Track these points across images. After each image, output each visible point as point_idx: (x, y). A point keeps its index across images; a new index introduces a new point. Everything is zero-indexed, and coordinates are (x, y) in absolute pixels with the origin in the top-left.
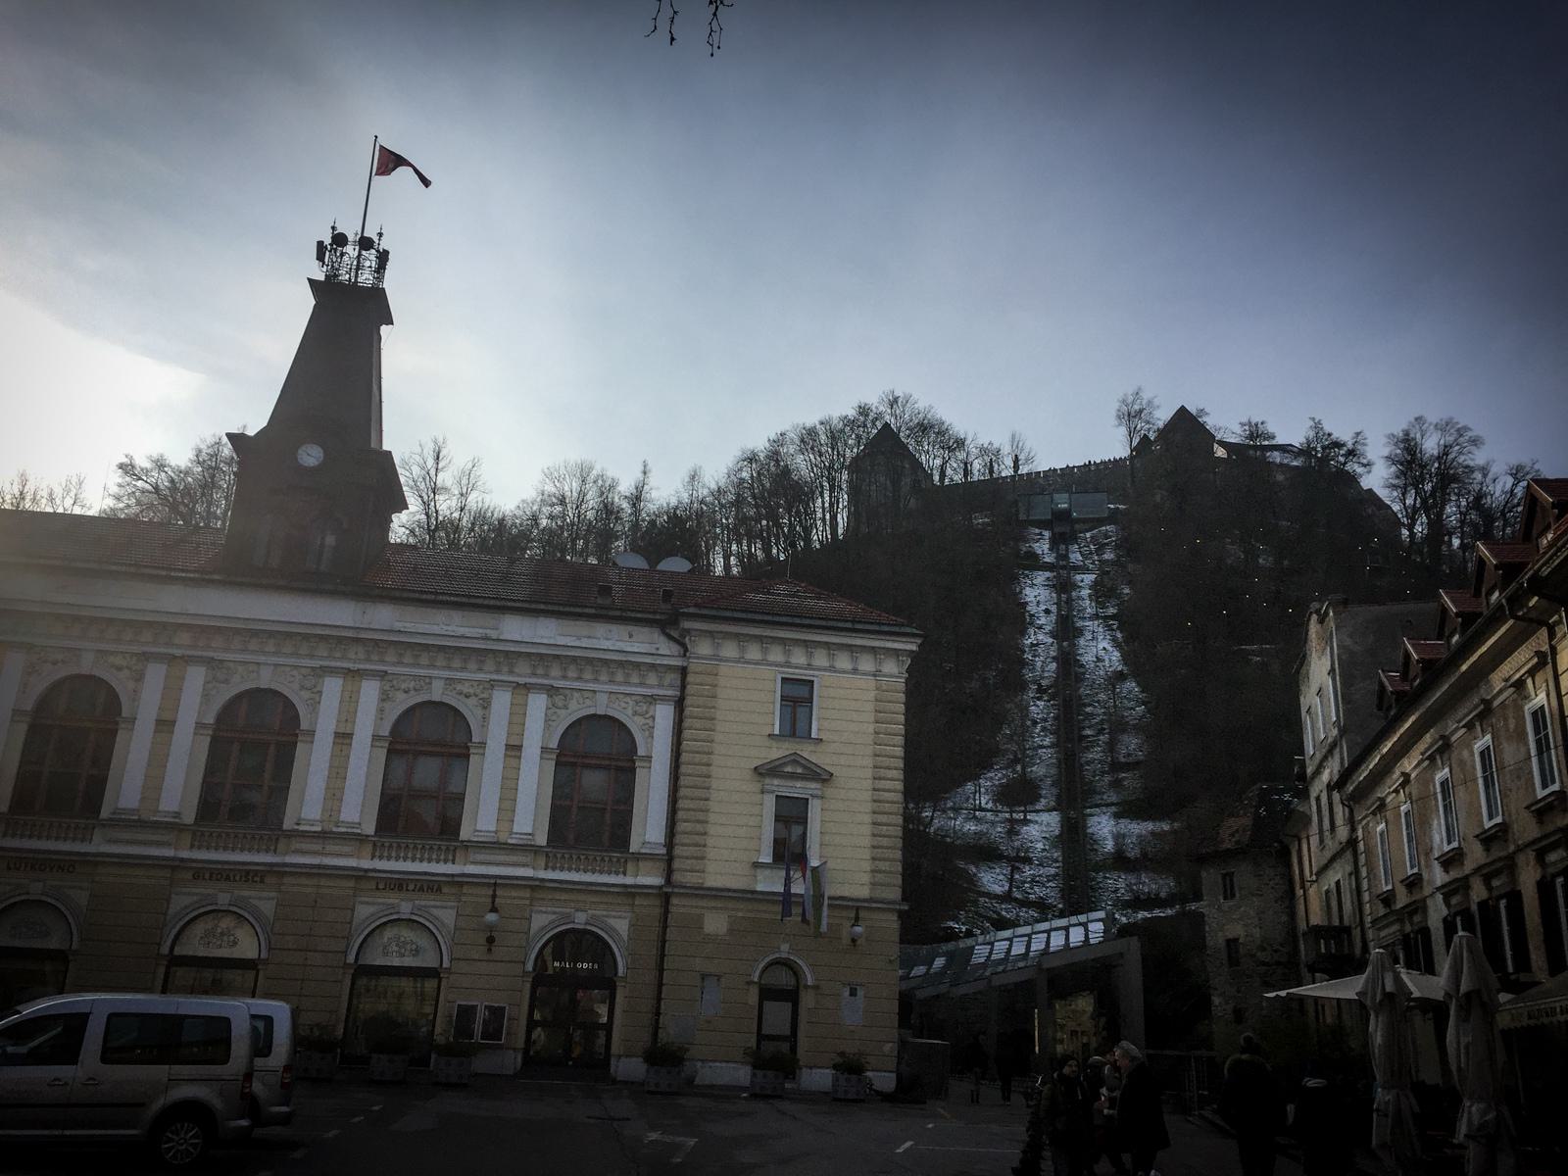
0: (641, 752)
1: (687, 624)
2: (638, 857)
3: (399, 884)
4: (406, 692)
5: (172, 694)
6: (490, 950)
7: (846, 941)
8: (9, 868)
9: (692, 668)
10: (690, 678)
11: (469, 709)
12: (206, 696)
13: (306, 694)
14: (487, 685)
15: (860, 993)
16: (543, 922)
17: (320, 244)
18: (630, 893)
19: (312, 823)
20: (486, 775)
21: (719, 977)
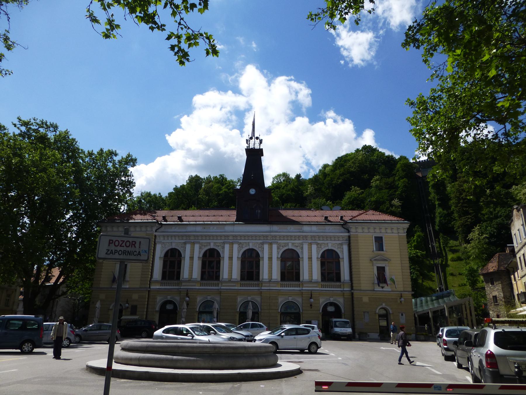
0: (341, 256)
7: (399, 302)
9: (351, 236)
10: (351, 239)
11: (298, 250)
12: (239, 252)
13: (260, 249)
15: (404, 315)
16: (323, 301)
17: (247, 140)
19: (266, 279)
21: (368, 313)
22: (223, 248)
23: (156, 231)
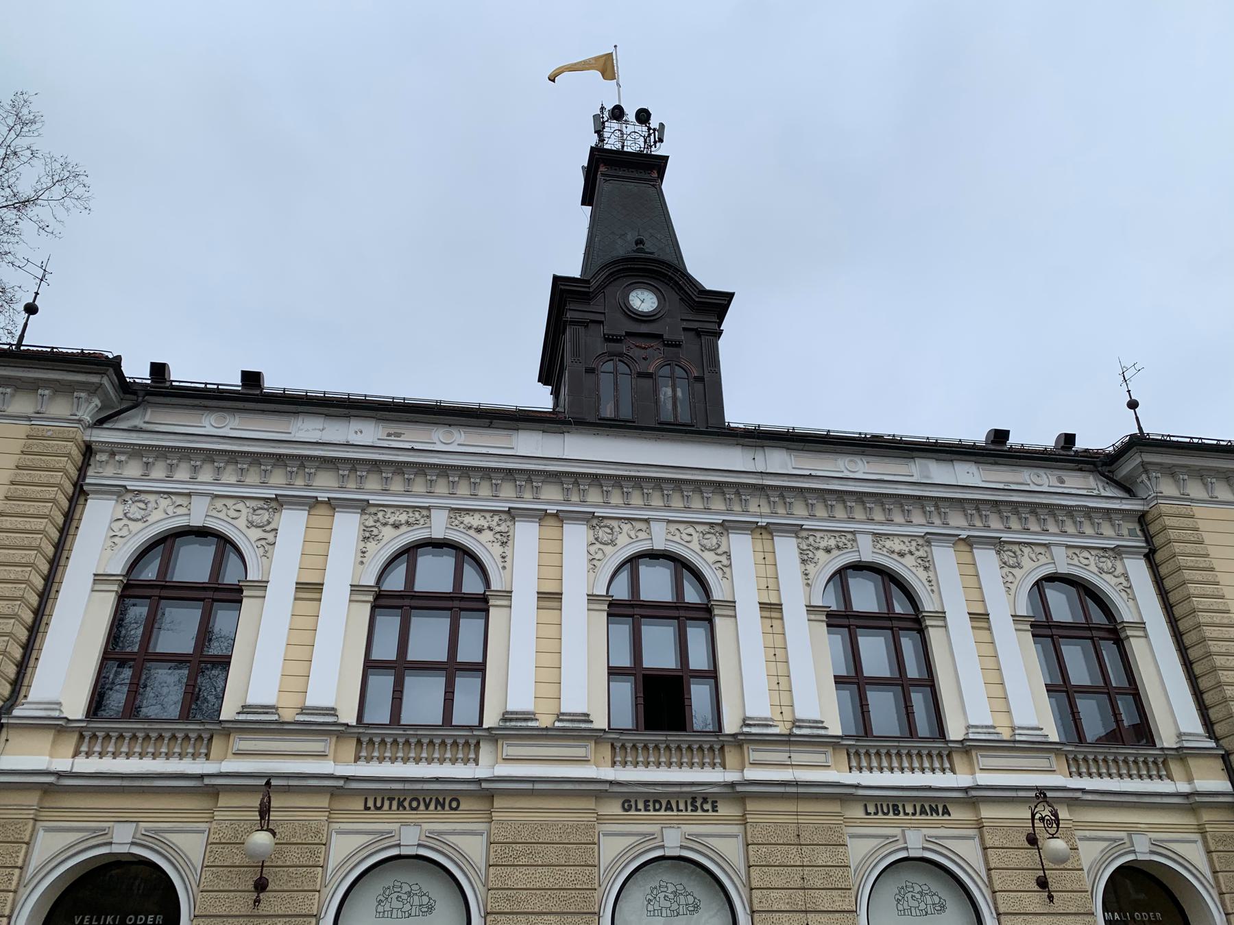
1: (1148, 458)
2: (1182, 754)
3: (891, 804)
4: (828, 551)
5: (552, 559)
6: (1051, 898)
8: (367, 808)
11: (907, 568)
13: (710, 557)
14: (921, 541)
18: (1192, 803)
20: (957, 656)
22: (505, 540)
23: (99, 423)
